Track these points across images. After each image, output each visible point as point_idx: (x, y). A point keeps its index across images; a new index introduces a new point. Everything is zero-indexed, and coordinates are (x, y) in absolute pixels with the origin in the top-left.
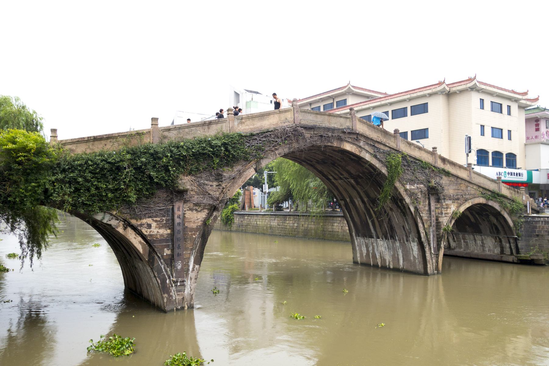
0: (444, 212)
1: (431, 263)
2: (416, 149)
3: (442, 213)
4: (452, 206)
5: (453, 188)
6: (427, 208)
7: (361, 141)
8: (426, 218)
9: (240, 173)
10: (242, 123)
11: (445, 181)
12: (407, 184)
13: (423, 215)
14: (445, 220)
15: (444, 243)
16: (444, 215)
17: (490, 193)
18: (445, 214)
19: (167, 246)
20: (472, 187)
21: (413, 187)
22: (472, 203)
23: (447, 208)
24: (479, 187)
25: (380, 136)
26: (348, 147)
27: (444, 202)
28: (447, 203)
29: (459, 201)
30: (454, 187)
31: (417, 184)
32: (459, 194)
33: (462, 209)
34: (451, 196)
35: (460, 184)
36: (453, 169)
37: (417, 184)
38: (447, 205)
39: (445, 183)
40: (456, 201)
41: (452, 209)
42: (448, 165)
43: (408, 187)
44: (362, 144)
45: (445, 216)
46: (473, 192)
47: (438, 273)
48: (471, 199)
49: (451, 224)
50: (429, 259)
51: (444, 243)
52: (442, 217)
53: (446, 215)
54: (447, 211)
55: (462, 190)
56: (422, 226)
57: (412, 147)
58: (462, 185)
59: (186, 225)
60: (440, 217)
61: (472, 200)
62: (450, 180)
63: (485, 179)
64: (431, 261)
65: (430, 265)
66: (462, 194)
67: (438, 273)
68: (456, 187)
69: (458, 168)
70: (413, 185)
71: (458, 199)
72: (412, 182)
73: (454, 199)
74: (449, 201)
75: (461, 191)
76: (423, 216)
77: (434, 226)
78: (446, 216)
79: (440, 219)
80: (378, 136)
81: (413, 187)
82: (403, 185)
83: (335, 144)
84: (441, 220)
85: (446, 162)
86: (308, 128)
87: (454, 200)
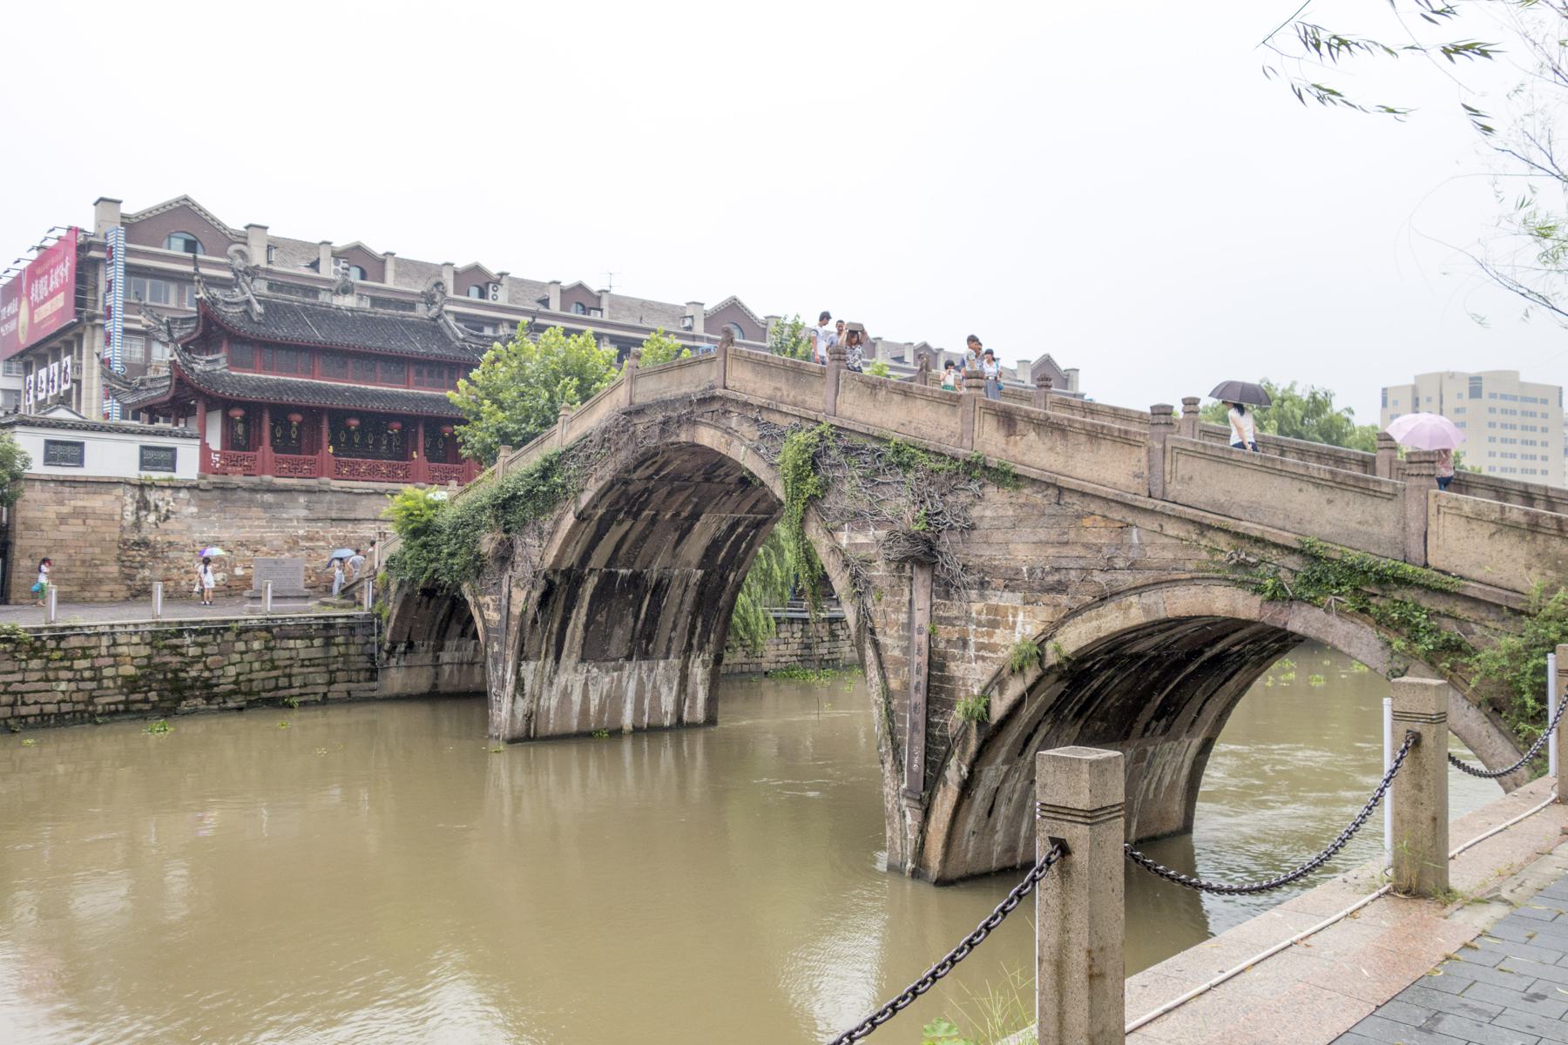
0: (972, 639)
1: (897, 826)
2: (895, 396)
3: (965, 644)
4: (1020, 617)
5: (1036, 539)
6: (903, 617)
7: (732, 414)
8: (897, 653)
9: (557, 523)
10: (571, 428)
11: (994, 505)
12: (843, 531)
13: (889, 641)
14: (971, 674)
15: (960, 769)
16: (972, 652)
17: (1293, 562)
18: (980, 647)
19: (496, 639)
20: (1156, 527)
21: (860, 539)
22: (1146, 610)
23: (994, 624)
24: (1203, 527)
25: (782, 385)
26: (707, 437)
27: (982, 597)
28: (994, 601)
29: (1064, 600)
30: (1042, 534)
31: (876, 529)
32: (1064, 563)
33: (1075, 638)
34: (1018, 571)
35: (1079, 517)
36: (1051, 449)
37: (876, 529)
38: (995, 610)
39: (993, 519)
40: (1046, 598)
41: (1019, 628)
42: (1032, 436)
43: (844, 538)
44: (734, 421)
45: (977, 658)
46: (1161, 554)
47: (915, 874)
48: (1138, 590)
49: (1001, 693)
50: (890, 806)
51: (960, 769)
52: (963, 657)
53: (982, 653)
54: (990, 635)
55: (1086, 546)
56: (877, 679)
57: (882, 394)
58: (1087, 522)
59: (511, 609)
60: (954, 658)
61: (1150, 598)
62: (1021, 501)
63: (1278, 481)
64: (897, 819)
65: (894, 830)
66: (1082, 563)
67: (915, 874)
68: (1054, 535)
69: (1083, 438)
70: (863, 528)
71: (1061, 588)
72: (857, 519)
73: (1036, 585)
74: (1007, 595)
75: (1079, 551)
76: (887, 645)
77: (917, 689)
78: (983, 659)
79: (952, 665)
80: (779, 385)
81: (860, 539)
82: (831, 532)
83: (683, 437)
84: (956, 669)
85: (1021, 426)
86: (640, 411)
87: (1031, 589)
